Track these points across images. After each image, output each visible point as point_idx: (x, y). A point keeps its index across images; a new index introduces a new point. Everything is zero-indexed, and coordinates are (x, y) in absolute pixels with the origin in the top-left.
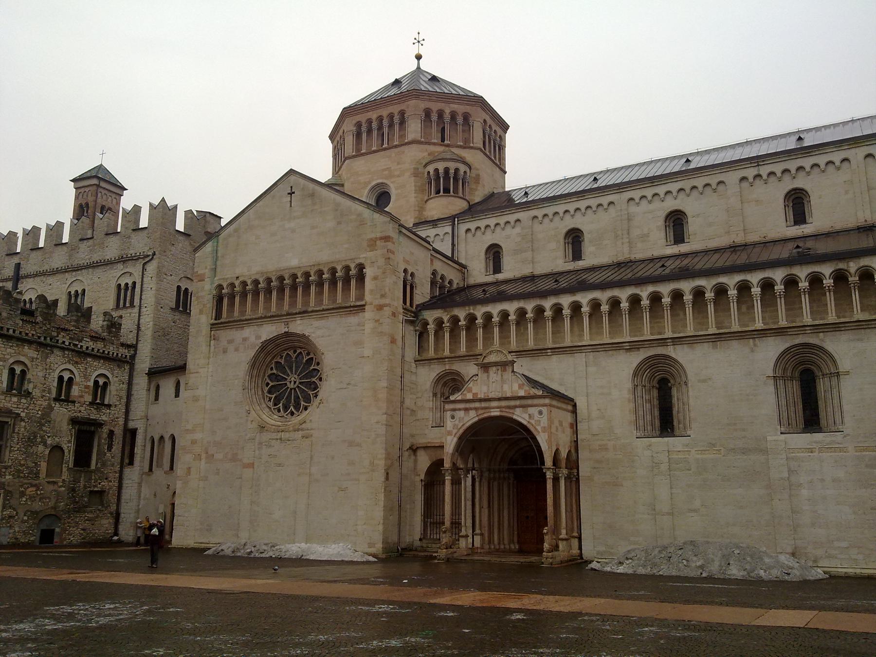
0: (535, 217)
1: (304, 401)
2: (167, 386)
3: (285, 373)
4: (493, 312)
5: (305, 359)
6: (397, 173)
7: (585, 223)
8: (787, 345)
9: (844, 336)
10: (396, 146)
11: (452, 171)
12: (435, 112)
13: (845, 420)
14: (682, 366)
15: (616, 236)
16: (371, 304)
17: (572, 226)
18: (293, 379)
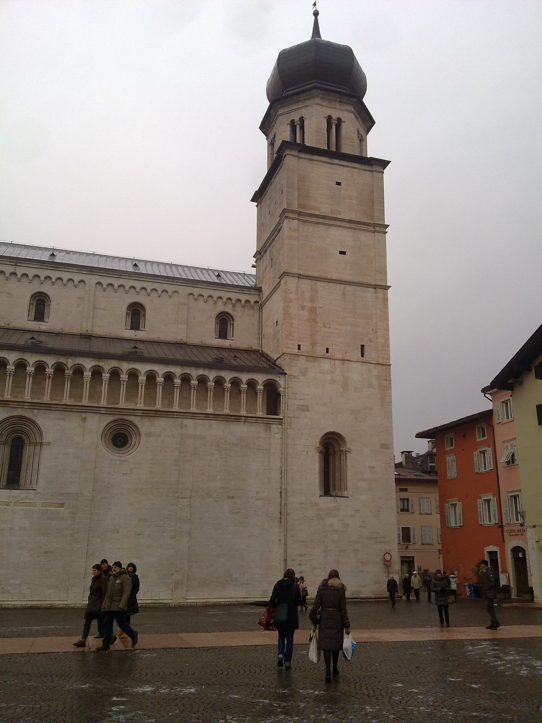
8: (7, 415)
9: (53, 415)
13: (39, 481)
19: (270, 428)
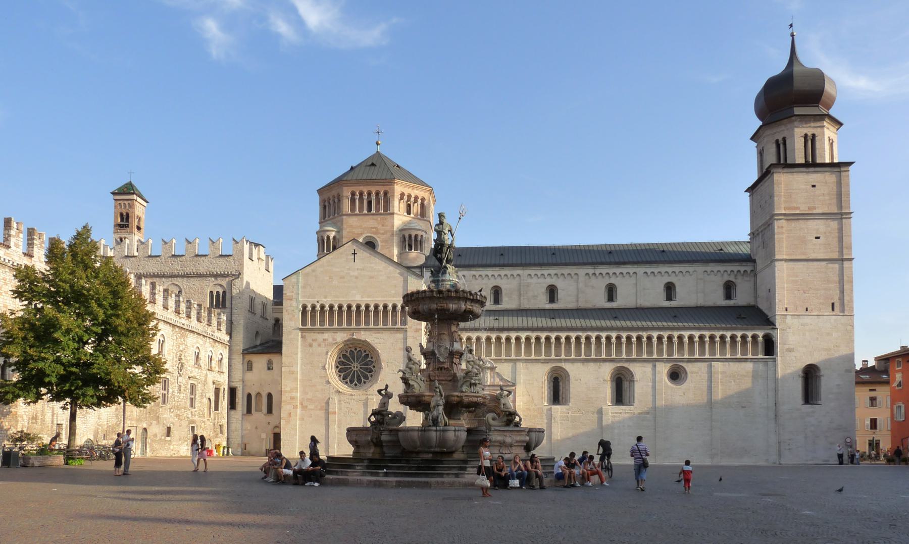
0: (474, 276)
1: (364, 378)
2: (260, 362)
3: (349, 361)
4: (472, 336)
5: (363, 355)
6: (382, 232)
7: (504, 284)
10: (381, 214)
11: (420, 237)
12: (406, 195)
14: (568, 373)
15: (520, 295)
16: (411, 328)
17: (495, 284)
18: (355, 365)
19: (767, 364)
